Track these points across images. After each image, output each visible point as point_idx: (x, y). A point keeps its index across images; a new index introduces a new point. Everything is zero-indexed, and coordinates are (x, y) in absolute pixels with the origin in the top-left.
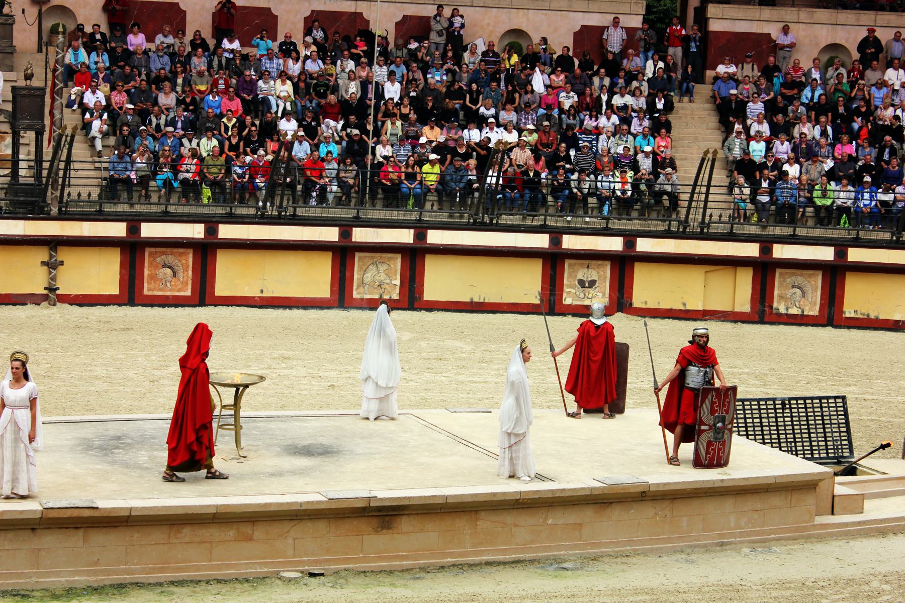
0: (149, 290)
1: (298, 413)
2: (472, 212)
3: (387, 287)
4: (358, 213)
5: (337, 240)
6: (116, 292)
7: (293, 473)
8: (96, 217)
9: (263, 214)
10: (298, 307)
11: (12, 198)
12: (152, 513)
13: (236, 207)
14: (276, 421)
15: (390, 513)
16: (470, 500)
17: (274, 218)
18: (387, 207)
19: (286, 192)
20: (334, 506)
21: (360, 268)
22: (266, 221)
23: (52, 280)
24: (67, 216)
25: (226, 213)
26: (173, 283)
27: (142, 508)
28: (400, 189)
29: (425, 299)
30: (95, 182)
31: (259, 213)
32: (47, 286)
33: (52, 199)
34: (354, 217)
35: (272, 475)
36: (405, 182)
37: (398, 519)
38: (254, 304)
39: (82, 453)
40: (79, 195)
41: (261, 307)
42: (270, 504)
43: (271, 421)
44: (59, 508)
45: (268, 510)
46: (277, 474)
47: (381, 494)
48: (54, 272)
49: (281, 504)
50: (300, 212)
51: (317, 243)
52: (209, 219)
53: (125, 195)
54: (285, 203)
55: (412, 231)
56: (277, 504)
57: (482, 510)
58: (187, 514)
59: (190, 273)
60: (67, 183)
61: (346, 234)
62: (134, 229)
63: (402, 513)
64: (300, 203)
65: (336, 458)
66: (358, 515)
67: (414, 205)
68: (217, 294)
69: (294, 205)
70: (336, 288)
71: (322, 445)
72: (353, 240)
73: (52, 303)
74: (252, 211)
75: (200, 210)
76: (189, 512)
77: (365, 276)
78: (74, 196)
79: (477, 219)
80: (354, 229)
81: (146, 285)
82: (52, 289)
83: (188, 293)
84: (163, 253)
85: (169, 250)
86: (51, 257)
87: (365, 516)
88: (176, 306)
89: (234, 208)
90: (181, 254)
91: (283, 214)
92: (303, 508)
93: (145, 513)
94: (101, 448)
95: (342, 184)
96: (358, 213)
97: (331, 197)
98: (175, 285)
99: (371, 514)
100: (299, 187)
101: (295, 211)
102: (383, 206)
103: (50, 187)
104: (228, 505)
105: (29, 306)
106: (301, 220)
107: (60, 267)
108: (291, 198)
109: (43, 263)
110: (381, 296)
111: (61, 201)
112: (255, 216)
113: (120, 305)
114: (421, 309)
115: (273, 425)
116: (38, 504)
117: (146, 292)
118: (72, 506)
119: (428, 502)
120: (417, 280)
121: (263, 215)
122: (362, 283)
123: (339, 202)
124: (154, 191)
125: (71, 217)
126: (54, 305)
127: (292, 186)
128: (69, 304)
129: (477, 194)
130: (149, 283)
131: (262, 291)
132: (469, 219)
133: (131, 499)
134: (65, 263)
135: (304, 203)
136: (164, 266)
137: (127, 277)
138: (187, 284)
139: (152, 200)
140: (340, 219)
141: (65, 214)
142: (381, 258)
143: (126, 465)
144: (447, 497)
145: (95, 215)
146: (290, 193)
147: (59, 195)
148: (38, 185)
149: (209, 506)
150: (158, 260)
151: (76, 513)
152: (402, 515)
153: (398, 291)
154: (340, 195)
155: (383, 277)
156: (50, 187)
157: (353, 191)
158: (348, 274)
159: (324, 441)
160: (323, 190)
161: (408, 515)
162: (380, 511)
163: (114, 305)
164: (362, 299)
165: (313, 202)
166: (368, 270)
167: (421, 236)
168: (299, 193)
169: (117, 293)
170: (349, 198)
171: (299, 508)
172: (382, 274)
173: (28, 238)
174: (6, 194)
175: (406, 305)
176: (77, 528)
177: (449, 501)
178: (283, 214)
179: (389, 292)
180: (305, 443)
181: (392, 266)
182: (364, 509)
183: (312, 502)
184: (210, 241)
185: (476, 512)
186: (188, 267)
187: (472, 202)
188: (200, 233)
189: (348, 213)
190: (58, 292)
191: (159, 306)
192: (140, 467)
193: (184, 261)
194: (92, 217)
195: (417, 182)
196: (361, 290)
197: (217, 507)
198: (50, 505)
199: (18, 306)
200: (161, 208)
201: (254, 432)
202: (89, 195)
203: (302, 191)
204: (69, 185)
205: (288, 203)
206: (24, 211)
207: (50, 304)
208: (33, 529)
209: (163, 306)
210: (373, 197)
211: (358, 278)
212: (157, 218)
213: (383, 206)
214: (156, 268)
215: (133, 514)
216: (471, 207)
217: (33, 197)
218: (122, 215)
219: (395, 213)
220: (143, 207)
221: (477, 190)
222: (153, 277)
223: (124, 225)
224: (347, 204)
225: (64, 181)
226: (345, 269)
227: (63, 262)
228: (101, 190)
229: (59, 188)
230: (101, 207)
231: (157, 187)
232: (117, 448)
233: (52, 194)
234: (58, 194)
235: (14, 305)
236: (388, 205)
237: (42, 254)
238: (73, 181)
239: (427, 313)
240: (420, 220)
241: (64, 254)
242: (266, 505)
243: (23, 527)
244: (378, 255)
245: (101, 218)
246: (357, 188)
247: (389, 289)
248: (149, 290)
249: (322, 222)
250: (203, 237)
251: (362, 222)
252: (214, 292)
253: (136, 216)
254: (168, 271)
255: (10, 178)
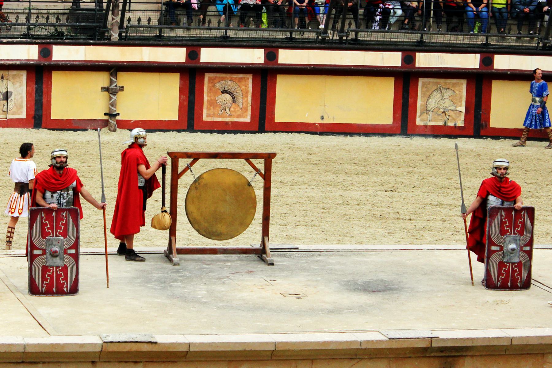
0: (208, 116)
1: (359, 247)
2: (543, 34)
3: (451, 113)
4: (422, 37)
5: (399, 64)
6: (176, 118)
7: (351, 309)
8: (156, 43)
9: (324, 39)
10: (359, 134)
11: (74, 24)
12: (210, 349)
13: (296, 31)
14: (336, 255)
15: (452, 355)
16: (536, 342)
17: (335, 43)
18: (451, 31)
19: (348, 16)
20: (394, 345)
21: (424, 94)
22: (326, 45)
23: (112, 106)
24: (127, 42)
25: (287, 38)
26: (232, 109)
27: (200, 343)
28: (466, 12)
29: (491, 126)
30: (154, 7)
31: (320, 38)
32: (107, 112)
33: (112, 25)
34: (418, 42)
35: (331, 312)
36: (471, 5)
37: (461, 361)
38: (314, 131)
39: (141, 286)
40: (139, 20)
41: (321, 134)
42: (329, 343)
43: (331, 255)
44: (119, 342)
45: (326, 348)
46: (336, 311)
47: (443, 335)
48: (114, 98)
49: (341, 343)
50: (362, 36)
51: (379, 69)
52: (269, 44)
53: (184, 20)
54: (346, 27)
55: (478, 56)
56: (336, 342)
57: (549, 353)
58: (245, 351)
59: (250, 98)
60: (127, 8)
61: (409, 59)
62: (193, 55)
63: (465, 354)
64: (362, 28)
65: (396, 295)
66: (419, 355)
67: (480, 30)
68: (276, 120)
69: (357, 30)
70: (399, 115)
71: (382, 281)
72: (417, 65)
73: (112, 129)
74: (313, 36)
75: (260, 35)
76: (247, 349)
77: (429, 102)
78: (134, 22)
79: (547, 43)
80: (417, 54)
81: (205, 111)
82: (112, 115)
83: (248, 119)
84: (223, 79)
85: (228, 76)
86: (111, 82)
87: (426, 357)
88: (235, 132)
89: (294, 33)
90: (240, 80)
91: (344, 38)
92: (363, 347)
93: (204, 349)
94: (160, 281)
95: (406, 8)
96: (422, 37)
97: (392, 20)
98: (235, 111)
99: (432, 355)
100: (361, 11)
101: (356, 35)
102: (448, 30)
103: (110, 12)
104: (287, 343)
105: (90, 131)
106: (362, 44)
107: (120, 93)
108: (353, 22)
109: (105, 89)
110: (445, 123)
111: (121, 27)
112: (315, 41)
113: (179, 131)
114: (487, 137)
115: (333, 259)
116: (98, 338)
117: (205, 118)
118: (131, 340)
119: (492, 343)
120: (483, 107)
121: (323, 41)
122: (426, 110)
123: (401, 26)
124: (215, 15)
125: (131, 42)
126: (114, 131)
127: (354, 10)
128: (128, 130)
129: (547, 17)
130: (208, 109)
131: (322, 118)
132: (539, 43)
133: (190, 334)
134: (125, 89)
135: (367, 28)
136: (224, 92)
137: (186, 103)
138: (246, 110)
139: (212, 25)
140: (403, 44)
141: (125, 40)
142: (446, 83)
143: (183, 298)
144: (512, 339)
145: (155, 40)
146: (352, 16)
147: (119, 20)
148: (98, 11)
149: (267, 343)
150: (218, 85)
151: (135, 348)
152: (465, 356)
153: (463, 117)
154: (403, 18)
155: (447, 103)
156: (110, 12)
157: (416, 15)
158: (411, 100)
159: (383, 276)
160: (386, 13)
161: (472, 356)
162: (442, 352)
163: (173, 131)
164: (426, 126)
165: (375, 26)
166: (432, 96)
167: (487, 61)
168: (361, 17)
169: (177, 120)
170: (412, 20)
171: (359, 347)
172: (447, 101)
173: (89, 64)
174: (67, 19)
175: (471, 133)
176: (136, 362)
177: (514, 343)
178: (344, 38)
179: (454, 119)
180: (367, 278)
181: (457, 92)
182: (425, 349)
183: (372, 341)
184: (270, 66)
185: (543, 355)
186: (247, 92)
187: (542, 25)
188: (260, 58)
189: (412, 38)
190: (118, 118)
191: (219, 132)
192: (199, 301)
193: (243, 87)
194: (151, 42)
195: (483, 5)
196: (425, 116)
197: (275, 344)
198: (110, 339)
199: (79, 132)
200: (221, 33)
201: (312, 266)
202: (149, 20)
203: (364, 15)
204: (130, 10)
205: (350, 27)
206: (86, 36)
207: (110, 130)
208: (93, 363)
209: (222, 132)
210: (438, 21)
211: (421, 105)
212: (217, 43)
213: (448, 30)
214: (216, 93)
215: (192, 349)
216: (540, 31)
217: (94, 22)
218: (182, 40)
219: (461, 37)
220: (202, 31)
221: (547, 12)
222: (212, 103)
223: (183, 50)
224: (412, 28)
225: (124, 6)
226: (408, 96)
227: (123, 87)
228: (161, 14)
229: (120, 12)
230: (160, 32)
231: (218, 11)
232: (175, 281)
233: (113, 19)
234: (118, 19)
235: (75, 130)
236: (453, 29)
237: (102, 79)
238: (133, 7)
239: (494, 141)
240: (486, 45)
241: (124, 79)
242: (324, 343)
243: (83, 360)
244: (442, 81)
245: (161, 43)
246: (420, 12)
247: (454, 116)
248: (208, 116)
249: (384, 47)
250: (263, 62)
251: (426, 46)
252: (274, 118)
253: (195, 41)
254: (228, 97)
255: (71, 4)
